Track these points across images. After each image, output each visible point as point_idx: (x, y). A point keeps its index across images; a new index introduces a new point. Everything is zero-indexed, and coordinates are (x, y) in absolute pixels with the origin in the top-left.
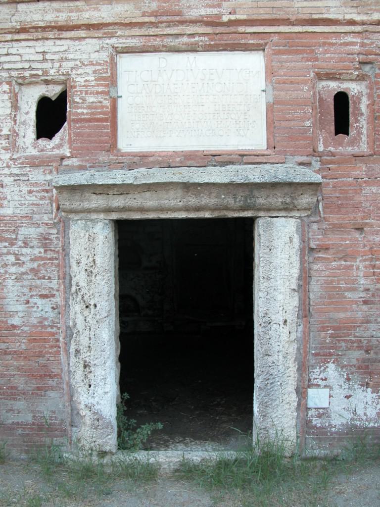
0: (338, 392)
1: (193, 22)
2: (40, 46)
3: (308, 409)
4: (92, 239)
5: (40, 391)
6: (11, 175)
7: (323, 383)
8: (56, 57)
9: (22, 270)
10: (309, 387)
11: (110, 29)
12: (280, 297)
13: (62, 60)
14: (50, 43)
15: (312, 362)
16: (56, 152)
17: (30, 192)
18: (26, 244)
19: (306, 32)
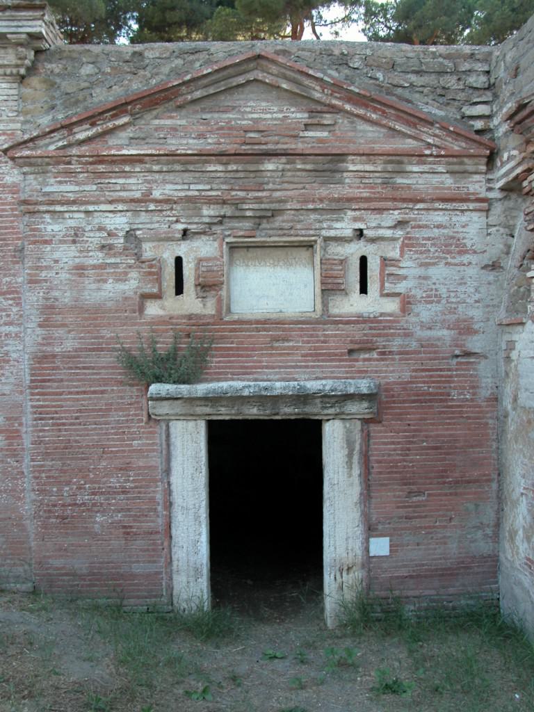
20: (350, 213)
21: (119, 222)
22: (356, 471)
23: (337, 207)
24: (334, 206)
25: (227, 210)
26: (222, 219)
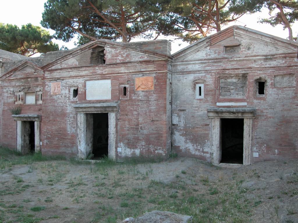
0: (123, 149)
1: (98, 75)
2: (73, 80)
3: (117, 152)
4: (81, 117)
5: (72, 146)
6: (69, 105)
7: (120, 147)
8: (76, 82)
9: (70, 123)
10: (118, 147)
11: (84, 76)
12: (112, 129)
13: (77, 82)
14: (75, 79)
15: (118, 142)
16: (76, 100)
17: (72, 108)
18: (71, 118)
19: (117, 75)
20: (39, 87)
21: (12, 89)
22: (39, 130)
23: (37, 86)
24: (37, 86)
25: (24, 87)
26: (24, 89)
